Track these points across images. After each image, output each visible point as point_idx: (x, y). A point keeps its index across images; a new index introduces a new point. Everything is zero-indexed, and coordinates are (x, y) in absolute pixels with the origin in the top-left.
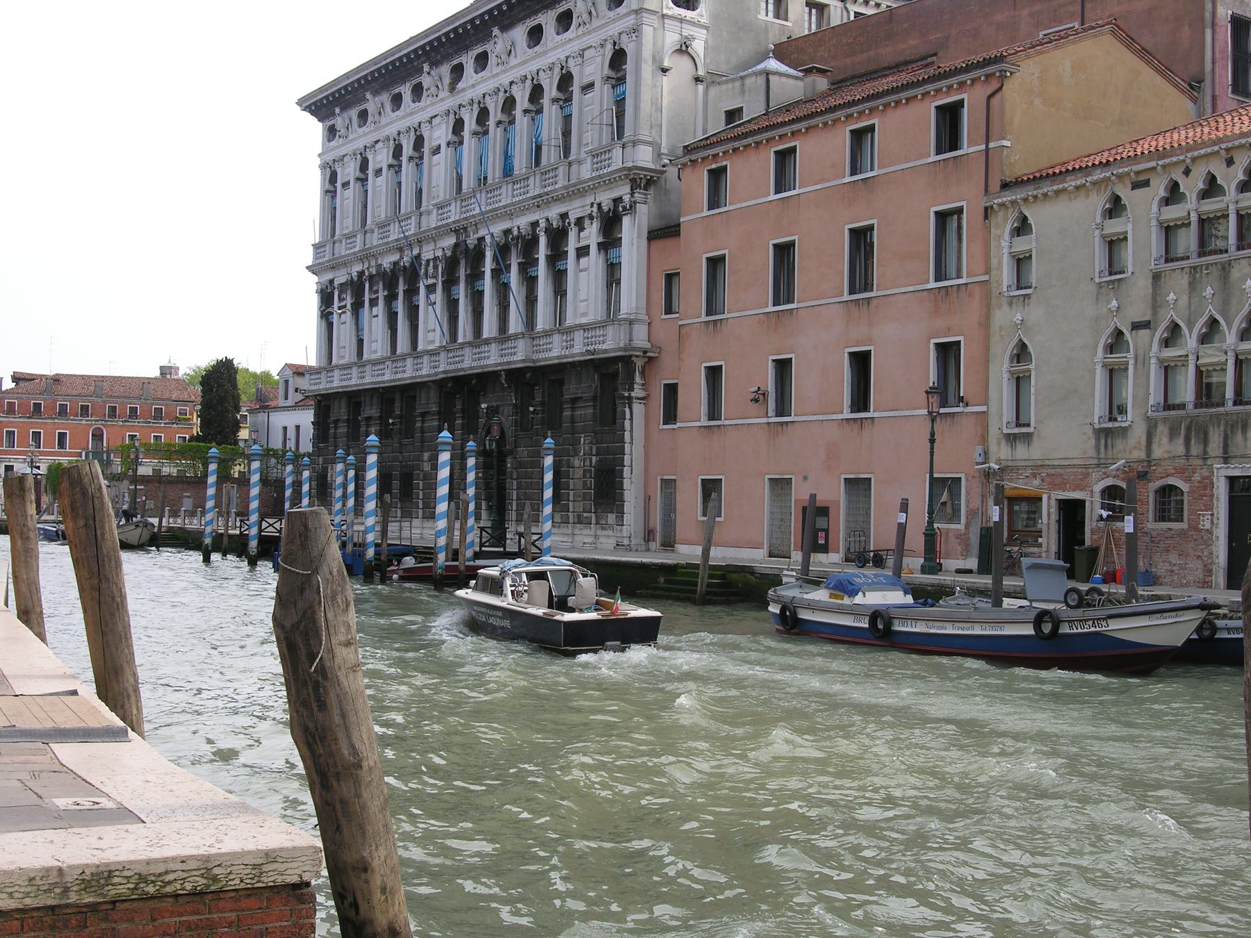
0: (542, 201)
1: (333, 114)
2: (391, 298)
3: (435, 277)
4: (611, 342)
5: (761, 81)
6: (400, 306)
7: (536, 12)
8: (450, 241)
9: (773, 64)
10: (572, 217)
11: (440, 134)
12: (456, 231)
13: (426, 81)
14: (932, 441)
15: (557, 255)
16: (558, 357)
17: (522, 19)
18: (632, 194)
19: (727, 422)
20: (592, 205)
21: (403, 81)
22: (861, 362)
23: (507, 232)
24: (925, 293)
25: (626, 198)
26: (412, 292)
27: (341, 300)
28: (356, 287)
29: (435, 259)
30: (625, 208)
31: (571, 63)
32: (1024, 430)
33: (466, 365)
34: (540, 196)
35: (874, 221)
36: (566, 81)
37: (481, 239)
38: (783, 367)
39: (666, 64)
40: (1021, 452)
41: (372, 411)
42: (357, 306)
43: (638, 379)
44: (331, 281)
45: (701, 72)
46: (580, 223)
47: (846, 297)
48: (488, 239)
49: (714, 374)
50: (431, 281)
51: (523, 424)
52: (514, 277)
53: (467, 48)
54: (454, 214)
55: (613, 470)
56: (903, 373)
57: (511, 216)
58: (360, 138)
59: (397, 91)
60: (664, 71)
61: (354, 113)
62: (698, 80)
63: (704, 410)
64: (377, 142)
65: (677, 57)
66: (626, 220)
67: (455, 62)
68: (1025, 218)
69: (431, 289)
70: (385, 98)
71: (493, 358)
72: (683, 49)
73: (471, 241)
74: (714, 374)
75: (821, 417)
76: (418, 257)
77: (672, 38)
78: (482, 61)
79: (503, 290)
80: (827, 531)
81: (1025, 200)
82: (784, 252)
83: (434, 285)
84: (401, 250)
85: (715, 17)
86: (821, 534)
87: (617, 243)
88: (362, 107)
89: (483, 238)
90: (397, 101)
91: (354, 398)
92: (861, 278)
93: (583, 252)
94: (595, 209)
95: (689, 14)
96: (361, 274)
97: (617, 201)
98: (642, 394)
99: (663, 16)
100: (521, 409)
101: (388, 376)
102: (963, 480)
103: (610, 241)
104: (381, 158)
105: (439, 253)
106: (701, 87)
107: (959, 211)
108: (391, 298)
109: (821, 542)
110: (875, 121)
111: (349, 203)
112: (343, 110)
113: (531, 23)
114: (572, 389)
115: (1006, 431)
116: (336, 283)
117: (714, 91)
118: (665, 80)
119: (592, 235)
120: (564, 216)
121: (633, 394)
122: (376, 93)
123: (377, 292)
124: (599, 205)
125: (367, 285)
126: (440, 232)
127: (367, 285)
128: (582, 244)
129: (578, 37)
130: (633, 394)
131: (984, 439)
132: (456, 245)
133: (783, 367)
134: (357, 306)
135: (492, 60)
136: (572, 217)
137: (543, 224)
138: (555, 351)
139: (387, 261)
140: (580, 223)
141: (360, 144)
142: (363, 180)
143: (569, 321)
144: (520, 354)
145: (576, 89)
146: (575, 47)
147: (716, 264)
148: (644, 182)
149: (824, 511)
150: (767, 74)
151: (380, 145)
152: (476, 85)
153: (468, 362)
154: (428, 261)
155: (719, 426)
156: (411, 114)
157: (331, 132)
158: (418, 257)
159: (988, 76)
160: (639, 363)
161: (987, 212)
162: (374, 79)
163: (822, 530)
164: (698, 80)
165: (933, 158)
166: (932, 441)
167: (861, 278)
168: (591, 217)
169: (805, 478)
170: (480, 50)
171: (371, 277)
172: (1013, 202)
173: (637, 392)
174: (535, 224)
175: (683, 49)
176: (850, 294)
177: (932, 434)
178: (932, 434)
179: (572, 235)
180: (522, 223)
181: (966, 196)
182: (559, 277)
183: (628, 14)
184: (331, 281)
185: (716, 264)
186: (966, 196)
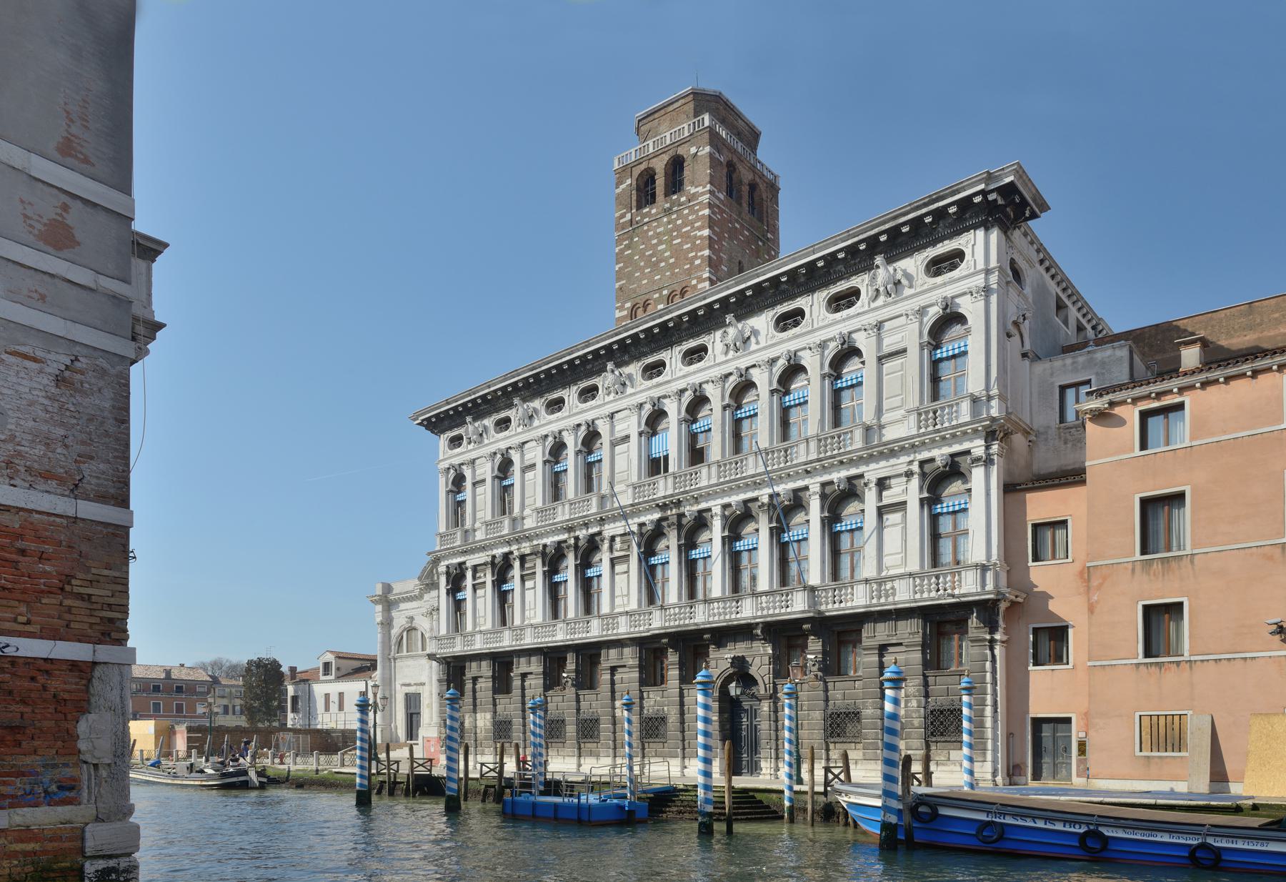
8: (657, 516)
12: (663, 507)
18: (988, 447)
20: (911, 462)
45: (1027, 346)
57: (757, 485)
62: (1024, 355)
66: (978, 474)
73: (690, 510)
89: (709, 510)
106: (1027, 362)
117: (1040, 368)
119: (912, 492)
137: (815, 488)
140: (882, 484)
146: (872, 319)
154: (613, 539)
158: (600, 533)
168: (909, 474)
179: (870, 496)
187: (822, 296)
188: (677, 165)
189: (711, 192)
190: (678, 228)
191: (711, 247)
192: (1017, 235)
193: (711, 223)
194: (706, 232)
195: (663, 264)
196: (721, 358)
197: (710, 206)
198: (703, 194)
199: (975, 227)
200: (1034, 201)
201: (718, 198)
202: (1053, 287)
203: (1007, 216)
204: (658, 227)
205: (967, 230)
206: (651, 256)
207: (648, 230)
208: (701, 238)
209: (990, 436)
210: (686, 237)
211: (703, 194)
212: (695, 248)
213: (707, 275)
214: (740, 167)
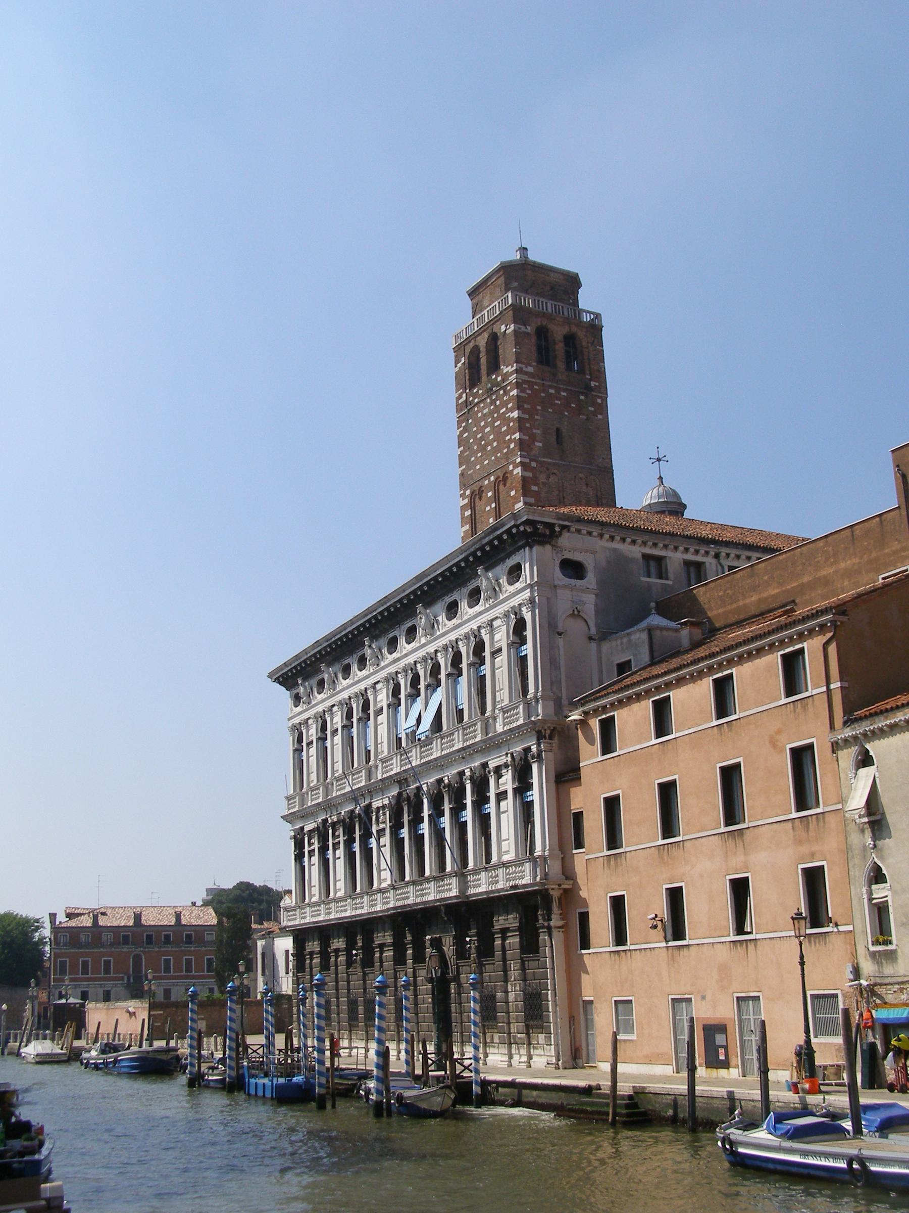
0: (466, 753)
1: (297, 684)
2: (349, 842)
3: (384, 822)
4: (526, 877)
5: (644, 636)
6: (357, 847)
7: (450, 591)
8: (394, 792)
9: (655, 620)
10: (492, 765)
11: (383, 698)
13: (368, 652)
14: (802, 963)
15: (481, 800)
16: (486, 892)
17: (441, 597)
18: (539, 745)
19: (632, 947)
20: (507, 754)
21: (351, 653)
22: (740, 888)
23: (440, 781)
24: (789, 824)
25: (534, 749)
26: (366, 835)
27: (310, 844)
28: (322, 833)
29: (384, 807)
30: (533, 757)
31: (483, 631)
32: (890, 947)
33: (410, 901)
34: (463, 749)
35: (740, 759)
36: (479, 648)
37: (419, 789)
38: (675, 896)
39: (560, 630)
40: (888, 970)
41: (339, 943)
42: (323, 849)
43: (555, 909)
44: (302, 828)
46: (498, 771)
47: (723, 829)
48: (425, 788)
49: (618, 904)
50: (382, 826)
51: (462, 953)
52: (446, 821)
53: (399, 623)
54: (396, 768)
55: (540, 994)
56: (777, 898)
57: (442, 768)
58: (321, 701)
59: (346, 662)
60: (560, 634)
61: (314, 681)
62: (591, 638)
63: (610, 936)
64: (333, 706)
65: (571, 622)
66: (535, 767)
67: (391, 635)
68: (867, 751)
69: (381, 832)
70: (337, 667)
71: (431, 894)
72: (576, 614)
74: (618, 904)
75: (711, 940)
76: (369, 806)
77: (563, 605)
78: (411, 633)
79: (438, 834)
80: (726, 1048)
81: (865, 735)
82: (667, 791)
83: (384, 829)
84: (356, 800)
85: (601, 583)
86: (722, 1051)
87: (529, 787)
88: (320, 677)
90: (347, 671)
91: (324, 932)
92: (732, 812)
93: (501, 796)
94: (509, 759)
95: (579, 582)
96: (325, 821)
97: (527, 750)
98: (560, 923)
99: (555, 586)
100: (460, 943)
101: (348, 912)
102: (840, 996)
103: (523, 785)
104: (337, 720)
105: (386, 802)
106: (594, 645)
107: (810, 747)
108: (349, 842)
109: (722, 1057)
110: (734, 670)
111: (313, 760)
112: (304, 680)
113: (448, 599)
114: (500, 922)
115: (872, 948)
116: (306, 829)
117: (606, 646)
118: (560, 641)
119: (508, 781)
120: (485, 765)
121: (552, 923)
122: (329, 664)
123: (338, 836)
124: (512, 754)
125: (330, 831)
126: (385, 784)
127: (330, 831)
128: (502, 789)
129: (487, 610)
130: (552, 923)
131: (854, 955)
132: (400, 794)
133: (675, 896)
134: (323, 849)
135: (420, 632)
136: (492, 765)
137: (468, 773)
138: (482, 886)
139: (344, 810)
140: (498, 771)
141: (320, 708)
142: (322, 739)
143: (494, 859)
144: (452, 890)
145: (487, 654)
147: (612, 805)
148: (548, 732)
149: (722, 1028)
150: (650, 630)
151: (335, 709)
152: (409, 653)
153: (412, 897)
154: (378, 808)
155: (625, 951)
156: (359, 680)
157: (297, 699)
159: (822, 626)
160: (555, 894)
161: (835, 747)
162: (328, 654)
163: (722, 1047)
164: (591, 638)
165: (784, 701)
166: (802, 963)
167: (732, 812)
168: (506, 766)
169: (703, 998)
170: (410, 624)
171: (334, 824)
172: (855, 738)
173: (555, 922)
174: (462, 773)
175: (576, 614)
176: (727, 825)
177: (802, 957)
178: (802, 957)
180: (449, 774)
181: (815, 732)
182: (484, 821)
183: (523, 589)
184: (302, 828)
185: (612, 805)
186: (815, 732)
187: (466, 591)
188: (494, 338)
189: (517, 371)
190: (497, 409)
191: (520, 429)
192: (565, 540)
193: (520, 403)
194: (515, 414)
195: (489, 448)
196: (423, 640)
197: (518, 385)
198: (512, 374)
199: (523, 547)
200: (559, 519)
201: (526, 373)
202: (635, 551)
203: (544, 535)
204: (484, 408)
205: (518, 549)
206: (482, 439)
207: (478, 412)
208: (513, 420)
209: (540, 737)
210: (502, 417)
211: (512, 374)
212: (510, 431)
213: (518, 460)
214: (552, 327)
